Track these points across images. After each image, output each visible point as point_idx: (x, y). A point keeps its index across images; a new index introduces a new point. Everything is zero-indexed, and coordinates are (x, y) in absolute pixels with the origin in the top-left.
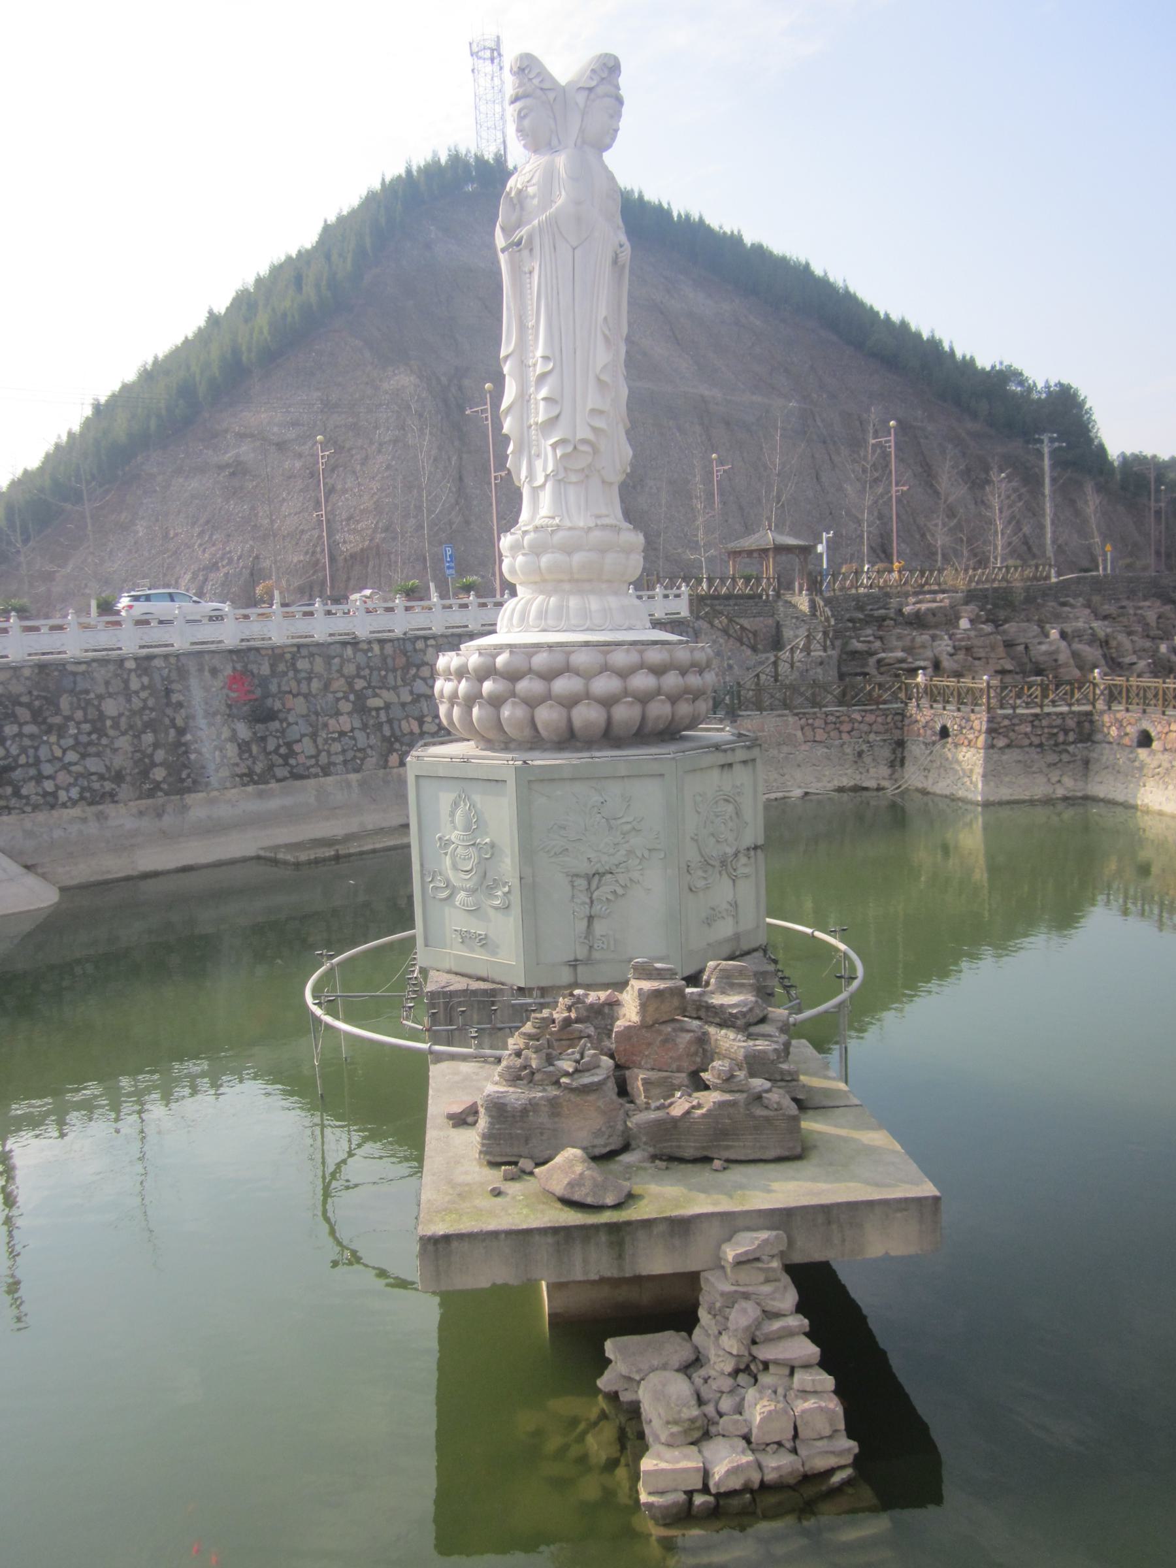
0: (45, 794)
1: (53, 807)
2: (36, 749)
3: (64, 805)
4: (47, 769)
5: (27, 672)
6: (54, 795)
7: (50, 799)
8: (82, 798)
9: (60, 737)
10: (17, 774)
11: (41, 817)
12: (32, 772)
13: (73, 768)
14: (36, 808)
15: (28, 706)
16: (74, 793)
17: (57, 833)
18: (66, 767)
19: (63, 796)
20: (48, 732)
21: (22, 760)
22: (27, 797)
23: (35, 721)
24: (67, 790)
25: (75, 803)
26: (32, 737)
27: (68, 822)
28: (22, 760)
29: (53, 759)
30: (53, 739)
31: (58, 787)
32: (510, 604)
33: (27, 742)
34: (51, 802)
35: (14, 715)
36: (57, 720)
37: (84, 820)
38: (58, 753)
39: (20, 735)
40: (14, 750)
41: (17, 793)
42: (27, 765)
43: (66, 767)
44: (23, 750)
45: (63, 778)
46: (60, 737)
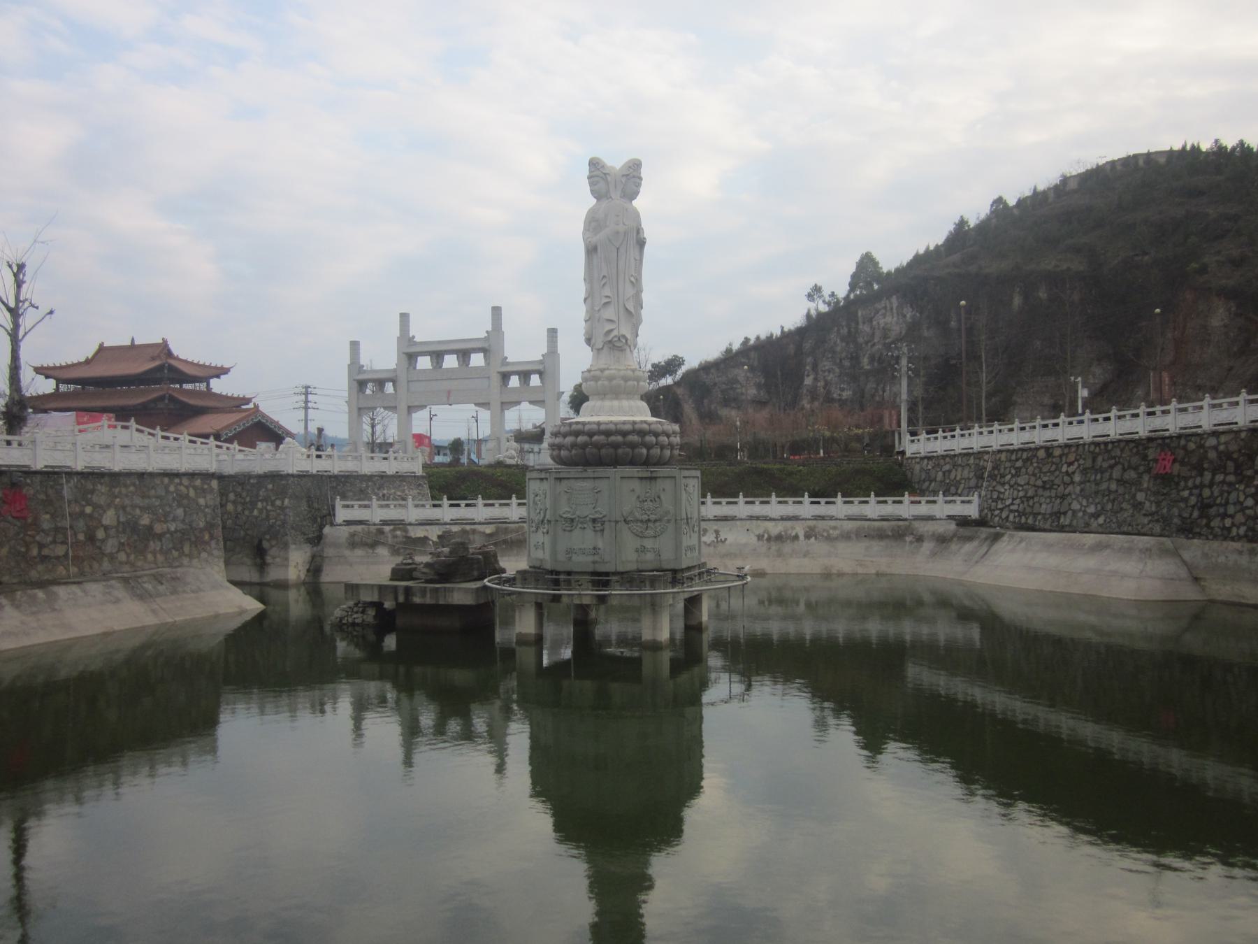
0: (1224, 528)
1: (1225, 539)
2: (1229, 493)
3: (1233, 539)
4: (1231, 510)
5: (1243, 435)
6: (1229, 529)
7: (1225, 532)
8: (1246, 536)
9: (1247, 486)
10: (1213, 511)
11: (1216, 544)
12: (1222, 510)
13: (1248, 512)
14: (1215, 537)
15: (1235, 461)
16: (1242, 530)
17: (1222, 559)
18: (1243, 510)
19: (1234, 531)
20: (1240, 482)
21: (1218, 501)
22: (1212, 528)
23: (1235, 473)
24: (1238, 528)
25: (1239, 538)
26: (1230, 484)
27: (1229, 553)
28: (1218, 501)
29: (1238, 502)
30: (1242, 487)
31: (1233, 524)
33: (1225, 488)
34: (1226, 535)
35: (1225, 467)
36: (1249, 473)
37: (1241, 553)
38: (1242, 498)
39: (1223, 482)
40: (1216, 494)
41: (1208, 525)
42: (1220, 505)
43: (1243, 510)
44: (1221, 495)
45: (1240, 518)
46: (1247, 486)
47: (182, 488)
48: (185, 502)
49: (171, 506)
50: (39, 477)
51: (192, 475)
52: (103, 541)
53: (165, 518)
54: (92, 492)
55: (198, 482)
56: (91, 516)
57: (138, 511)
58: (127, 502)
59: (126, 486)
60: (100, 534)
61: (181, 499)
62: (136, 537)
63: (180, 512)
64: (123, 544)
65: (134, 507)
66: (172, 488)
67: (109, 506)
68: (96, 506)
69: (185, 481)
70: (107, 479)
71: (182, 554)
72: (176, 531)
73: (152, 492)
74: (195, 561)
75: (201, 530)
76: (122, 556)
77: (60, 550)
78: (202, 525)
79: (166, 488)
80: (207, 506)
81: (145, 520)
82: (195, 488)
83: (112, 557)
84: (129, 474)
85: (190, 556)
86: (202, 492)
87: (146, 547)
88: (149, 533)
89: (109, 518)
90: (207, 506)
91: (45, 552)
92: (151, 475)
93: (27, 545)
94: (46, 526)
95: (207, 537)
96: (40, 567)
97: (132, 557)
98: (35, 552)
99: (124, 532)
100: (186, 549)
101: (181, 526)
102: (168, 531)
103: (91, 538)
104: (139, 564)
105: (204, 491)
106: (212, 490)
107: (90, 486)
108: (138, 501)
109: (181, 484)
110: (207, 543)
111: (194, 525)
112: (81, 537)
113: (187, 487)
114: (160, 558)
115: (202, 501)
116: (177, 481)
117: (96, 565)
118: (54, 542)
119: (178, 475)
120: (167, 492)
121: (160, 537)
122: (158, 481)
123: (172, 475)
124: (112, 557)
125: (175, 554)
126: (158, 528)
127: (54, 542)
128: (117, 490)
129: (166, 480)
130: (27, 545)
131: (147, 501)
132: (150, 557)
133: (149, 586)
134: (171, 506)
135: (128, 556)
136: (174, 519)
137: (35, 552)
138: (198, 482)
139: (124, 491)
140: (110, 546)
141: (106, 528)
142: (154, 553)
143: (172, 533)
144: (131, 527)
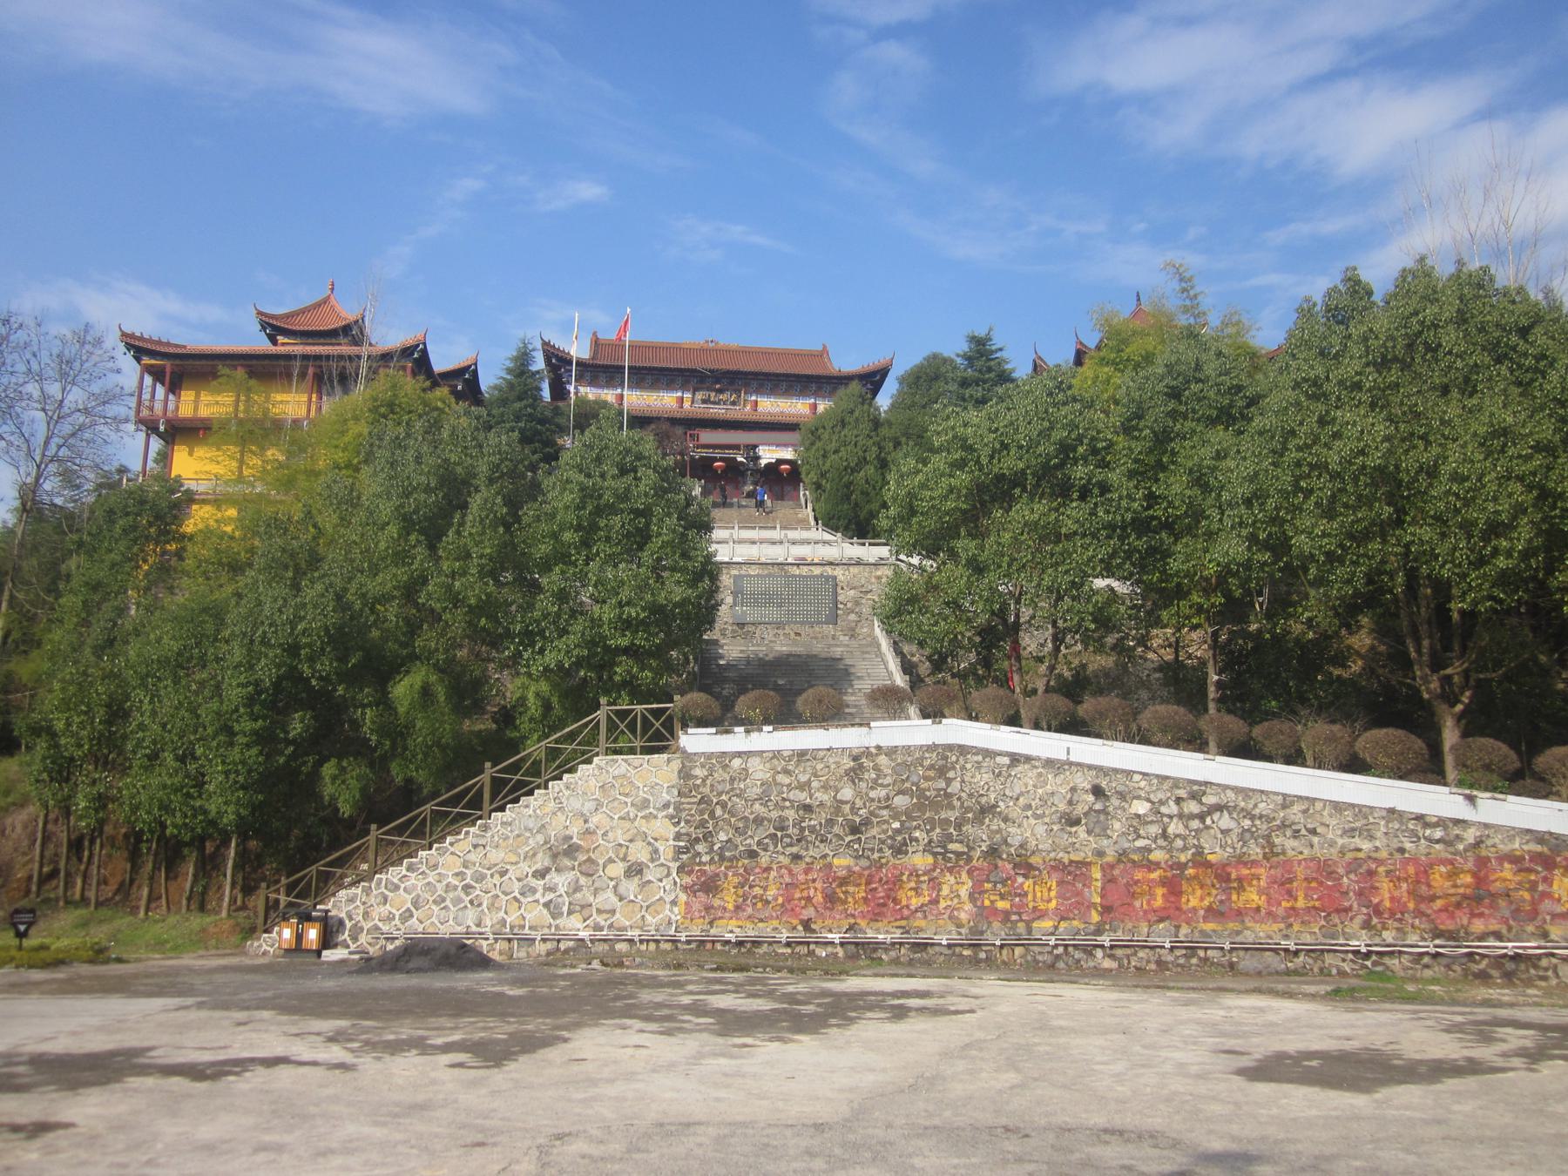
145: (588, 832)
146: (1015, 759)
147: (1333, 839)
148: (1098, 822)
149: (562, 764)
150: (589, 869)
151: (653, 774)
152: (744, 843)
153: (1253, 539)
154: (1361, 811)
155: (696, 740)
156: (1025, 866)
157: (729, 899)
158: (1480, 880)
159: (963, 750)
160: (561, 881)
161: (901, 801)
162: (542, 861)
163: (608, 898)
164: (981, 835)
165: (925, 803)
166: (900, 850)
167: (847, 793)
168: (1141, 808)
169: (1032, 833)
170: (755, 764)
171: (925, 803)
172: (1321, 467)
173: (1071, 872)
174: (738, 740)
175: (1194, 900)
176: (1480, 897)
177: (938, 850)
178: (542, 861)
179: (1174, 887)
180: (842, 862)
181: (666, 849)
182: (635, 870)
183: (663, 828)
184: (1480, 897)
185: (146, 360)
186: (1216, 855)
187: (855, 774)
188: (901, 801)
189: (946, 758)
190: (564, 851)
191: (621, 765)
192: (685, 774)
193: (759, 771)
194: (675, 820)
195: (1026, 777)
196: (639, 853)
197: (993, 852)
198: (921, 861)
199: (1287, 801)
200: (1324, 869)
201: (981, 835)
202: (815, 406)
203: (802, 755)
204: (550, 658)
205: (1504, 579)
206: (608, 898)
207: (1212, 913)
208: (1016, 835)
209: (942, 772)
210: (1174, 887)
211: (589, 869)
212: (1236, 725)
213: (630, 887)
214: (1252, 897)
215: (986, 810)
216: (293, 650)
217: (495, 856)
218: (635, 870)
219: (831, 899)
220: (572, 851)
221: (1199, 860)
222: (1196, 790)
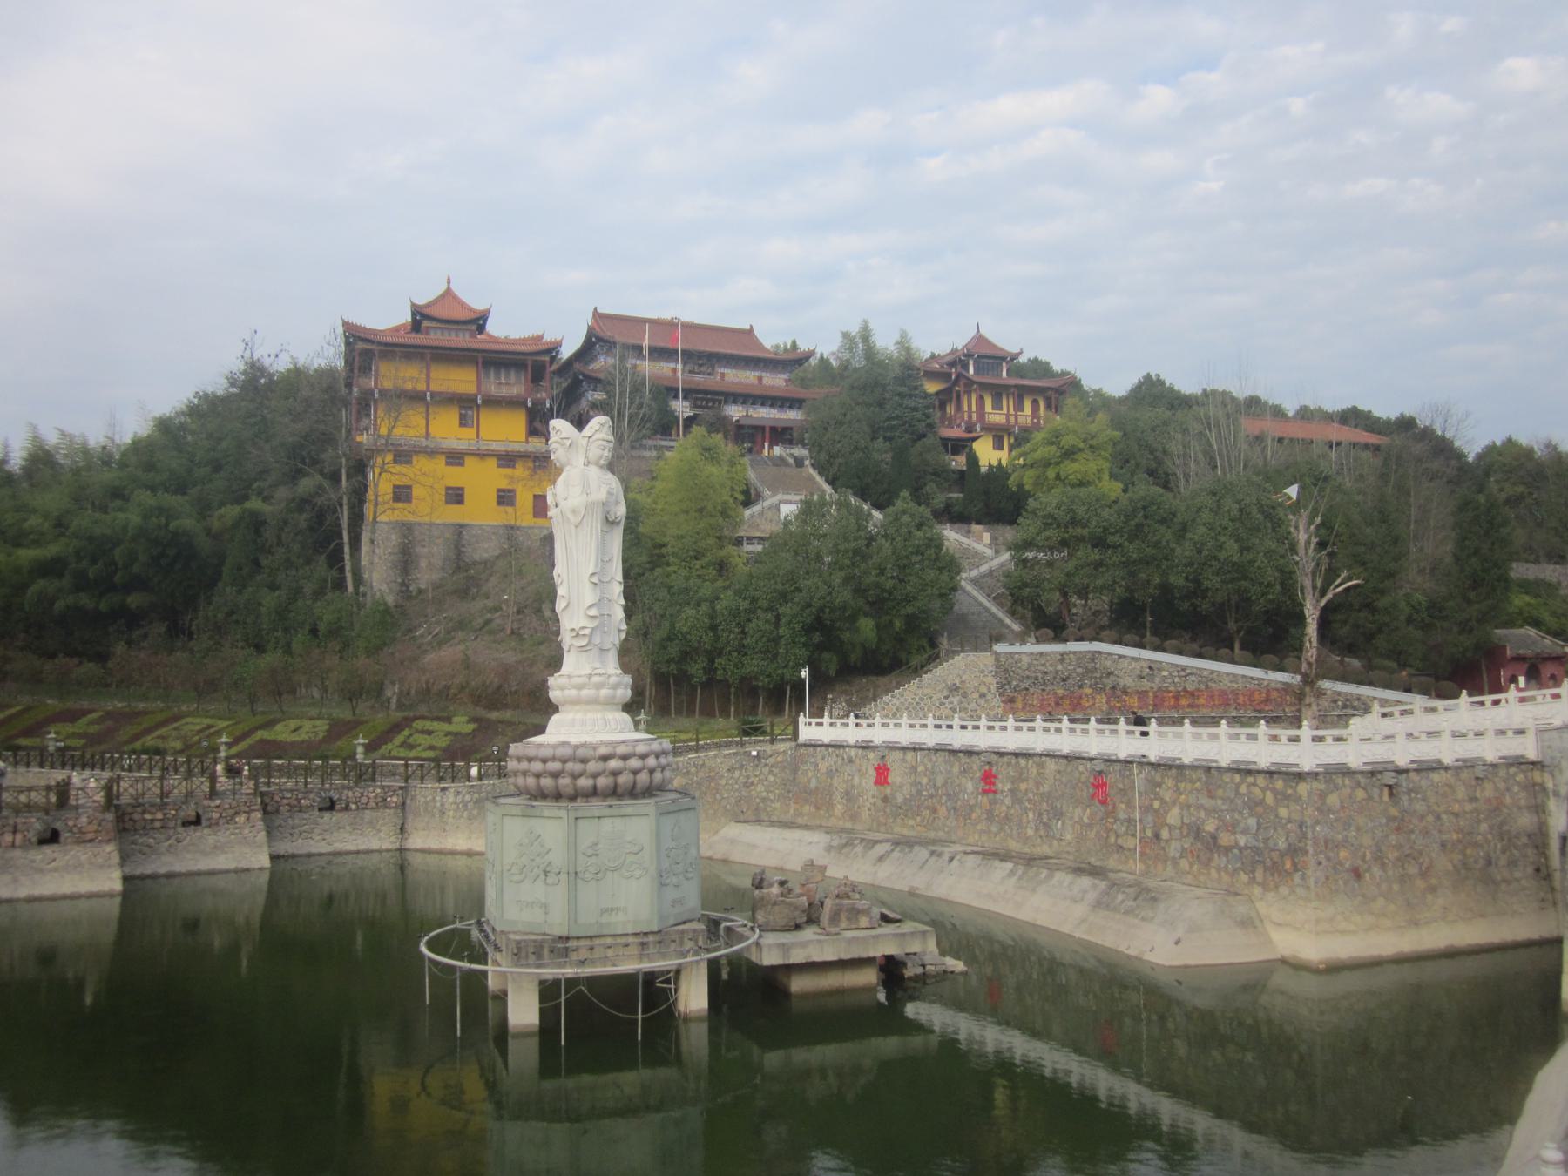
32: (555, 718)
47: (1257, 791)
48: (1259, 809)
49: (1241, 813)
50: (1118, 767)
51: (1270, 773)
52: (1167, 841)
53: (1232, 828)
54: (1159, 785)
55: (1279, 784)
56: (1156, 811)
57: (1202, 814)
58: (1192, 800)
59: (1192, 782)
60: (1165, 834)
61: (1254, 804)
62: (1199, 845)
63: (1252, 822)
64: (1184, 850)
65: (1201, 806)
66: (1243, 789)
67: (1174, 803)
68: (1163, 802)
69: (1261, 780)
70: (1174, 771)
71: (1253, 880)
72: (1246, 847)
73: (1220, 792)
74: (1270, 895)
75: (1282, 855)
76: (1184, 864)
77: (1130, 843)
78: (1282, 845)
79: (1238, 786)
80: (1289, 821)
81: (1210, 826)
82: (1275, 792)
83: (1175, 863)
84: (1193, 767)
85: (1264, 886)
86: (1282, 798)
87: (1210, 860)
88: (1212, 843)
89: (1173, 817)
90: (1289, 821)
91: (1120, 841)
92: (1219, 769)
93: (1108, 831)
94: (1122, 816)
95: (1288, 865)
96: (1116, 856)
97: (1195, 868)
98: (1112, 840)
99: (1188, 835)
100: (1259, 875)
101: (1254, 843)
102: (1236, 845)
103: (1157, 836)
104: (1202, 878)
105: (1287, 797)
106: (1298, 799)
107: (1158, 779)
108: (1205, 801)
109: (1254, 784)
110: (1289, 874)
111: (1271, 844)
112: (1149, 833)
113: (1263, 790)
114: (1226, 878)
115: (1283, 812)
116: (1250, 779)
117: (1160, 866)
118: (1126, 833)
119: (1249, 772)
120: (1238, 793)
121: (1228, 850)
122: (1227, 778)
123: (1244, 771)
124: (1175, 863)
125: (1244, 877)
126: (1225, 839)
127: (1126, 833)
128: (1182, 785)
129: (1237, 778)
130: (1108, 831)
131: (1212, 802)
132: (1213, 872)
133: (1120, 897)
134: (1241, 813)
135: (1191, 866)
136: (1245, 832)
137: (1112, 840)
138: (1279, 784)
139: (1189, 786)
140: (1174, 849)
141: (1170, 827)
142: (1218, 870)
143: (1241, 850)
144: (1196, 831)
145: (963, 682)
146: (1120, 657)
147: (1226, 684)
148: (1151, 678)
149: (952, 654)
150: (965, 695)
151: (984, 660)
152: (1023, 685)
153: (1187, 578)
154: (1235, 675)
155: (1001, 648)
156: (1125, 692)
157: (1019, 705)
158: (1268, 695)
159: (1100, 653)
160: (955, 700)
161: (1079, 670)
162: (946, 693)
163: (973, 705)
164: (1109, 682)
165: (1088, 671)
166: (1081, 687)
167: (1060, 667)
168: (1165, 673)
169: (1129, 681)
170: (1026, 660)
171: (1088, 671)
172: (1215, 558)
173: (1142, 694)
174: (1017, 648)
175: (1183, 702)
176: (1267, 700)
177: (1094, 687)
178: (946, 693)
179: (1177, 698)
180: (1060, 692)
181: (993, 688)
182: (983, 695)
183: (990, 679)
184: (1267, 700)
185: (361, 345)
186: (1190, 688)
187: (1062, 660)
188: (1079, 670)
189: (1095, 656)
190: (954, 689)
191: (972, 656)
192: (997, 660)
193: (1026, 660)
194: (996, 676)
195: (1124, 663)
196: (984, 689)
197: (1114, 688)
198: (1088, 691)
199: (1212, 672)
200: (1223, 693)
201: (1109, 682)
202: (760, 379)
203: (1041, 654)
204: (910, 610)
205: (1271, 601)
206: (973, 705)
207: (1190, 706)
208: (1122, 682)
209: (1093, 660)
210: (1177, 698)
211: (965, 695)
212: (1156, 640)
213: (982, 702)
214: (1202, 701)
215: (1110, 674)
216: (822, 609)
217: (927, 691)
218: (983, 695)
219: (1057, 704)
220: (957, 689)
221: (1185, 690)
222: (1184, 668)
